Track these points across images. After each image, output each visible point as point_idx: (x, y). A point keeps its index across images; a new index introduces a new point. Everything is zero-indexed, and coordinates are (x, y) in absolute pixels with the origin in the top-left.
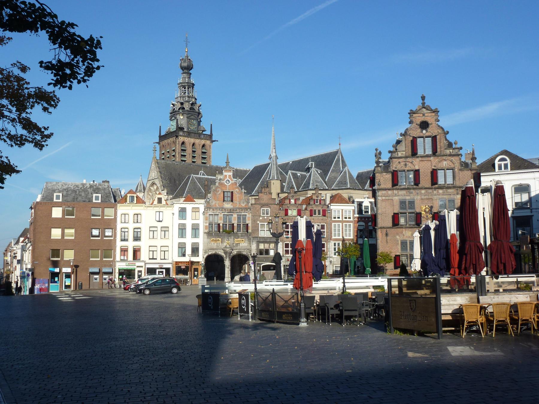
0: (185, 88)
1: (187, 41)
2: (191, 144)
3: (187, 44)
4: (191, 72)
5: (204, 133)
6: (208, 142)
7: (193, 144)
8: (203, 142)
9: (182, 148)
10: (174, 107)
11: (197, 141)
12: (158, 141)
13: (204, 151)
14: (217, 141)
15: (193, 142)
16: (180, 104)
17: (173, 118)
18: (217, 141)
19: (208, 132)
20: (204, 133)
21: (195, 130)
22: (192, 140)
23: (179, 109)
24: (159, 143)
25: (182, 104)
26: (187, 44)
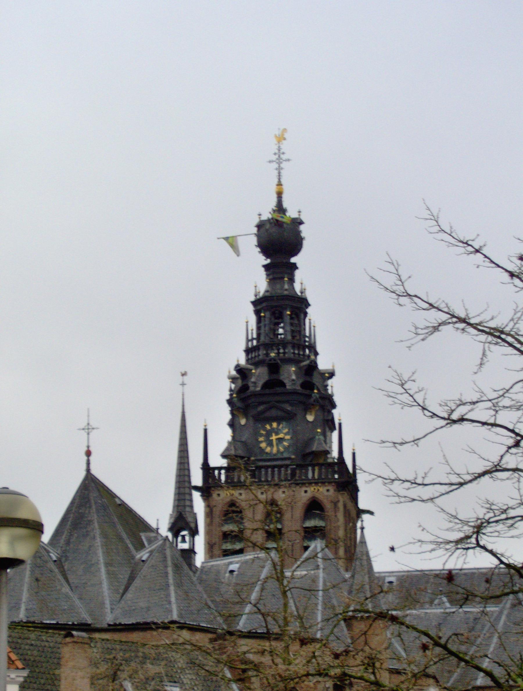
21: (286, 455)
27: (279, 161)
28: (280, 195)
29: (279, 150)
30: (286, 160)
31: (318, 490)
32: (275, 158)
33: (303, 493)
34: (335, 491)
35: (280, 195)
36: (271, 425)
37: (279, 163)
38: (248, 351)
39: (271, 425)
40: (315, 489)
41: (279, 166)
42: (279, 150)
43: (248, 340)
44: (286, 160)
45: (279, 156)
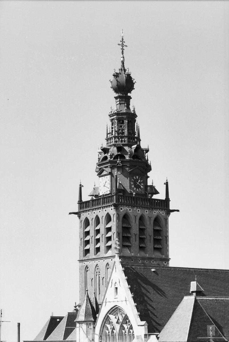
0: (123, 123)
1: (123, 45)
2: (138, 218)
3: (123, 49)
4: (129, 94)
5: (155, 197)
6: (162, 213)
7: (142, 218)
8: (156, 213)
9: (124, 226)
10: (106, 155)
11: (146, 213)
12: (77, 210)
13: (158, 228)
14: (178, 211)
15: (140, 214)
16: (115, 149)
17: (104, 173)
18: (178, 211)
19: (161, 196)
20: (155, 197)
22: (139, 212)
23: (116, 157)
24: (78, 214)
25: (120, 149)
26: (123, 49)
27: (123, 45)
28: (123, 63)
29: (123, 40)
30: (125, 46)
31: (160, 212)
32: (121, 43)
33: (154, 213)
34: (166, 213)
35: (123, 63)
36: (136, 177)
37: (123, 46)
38: (108, 139)
39: (136, 177)
40: (158, 212)
41: (123, 48)
42: (123, 40)
43: (108, 134)
44: (125, 46)
45: (123, 43)
